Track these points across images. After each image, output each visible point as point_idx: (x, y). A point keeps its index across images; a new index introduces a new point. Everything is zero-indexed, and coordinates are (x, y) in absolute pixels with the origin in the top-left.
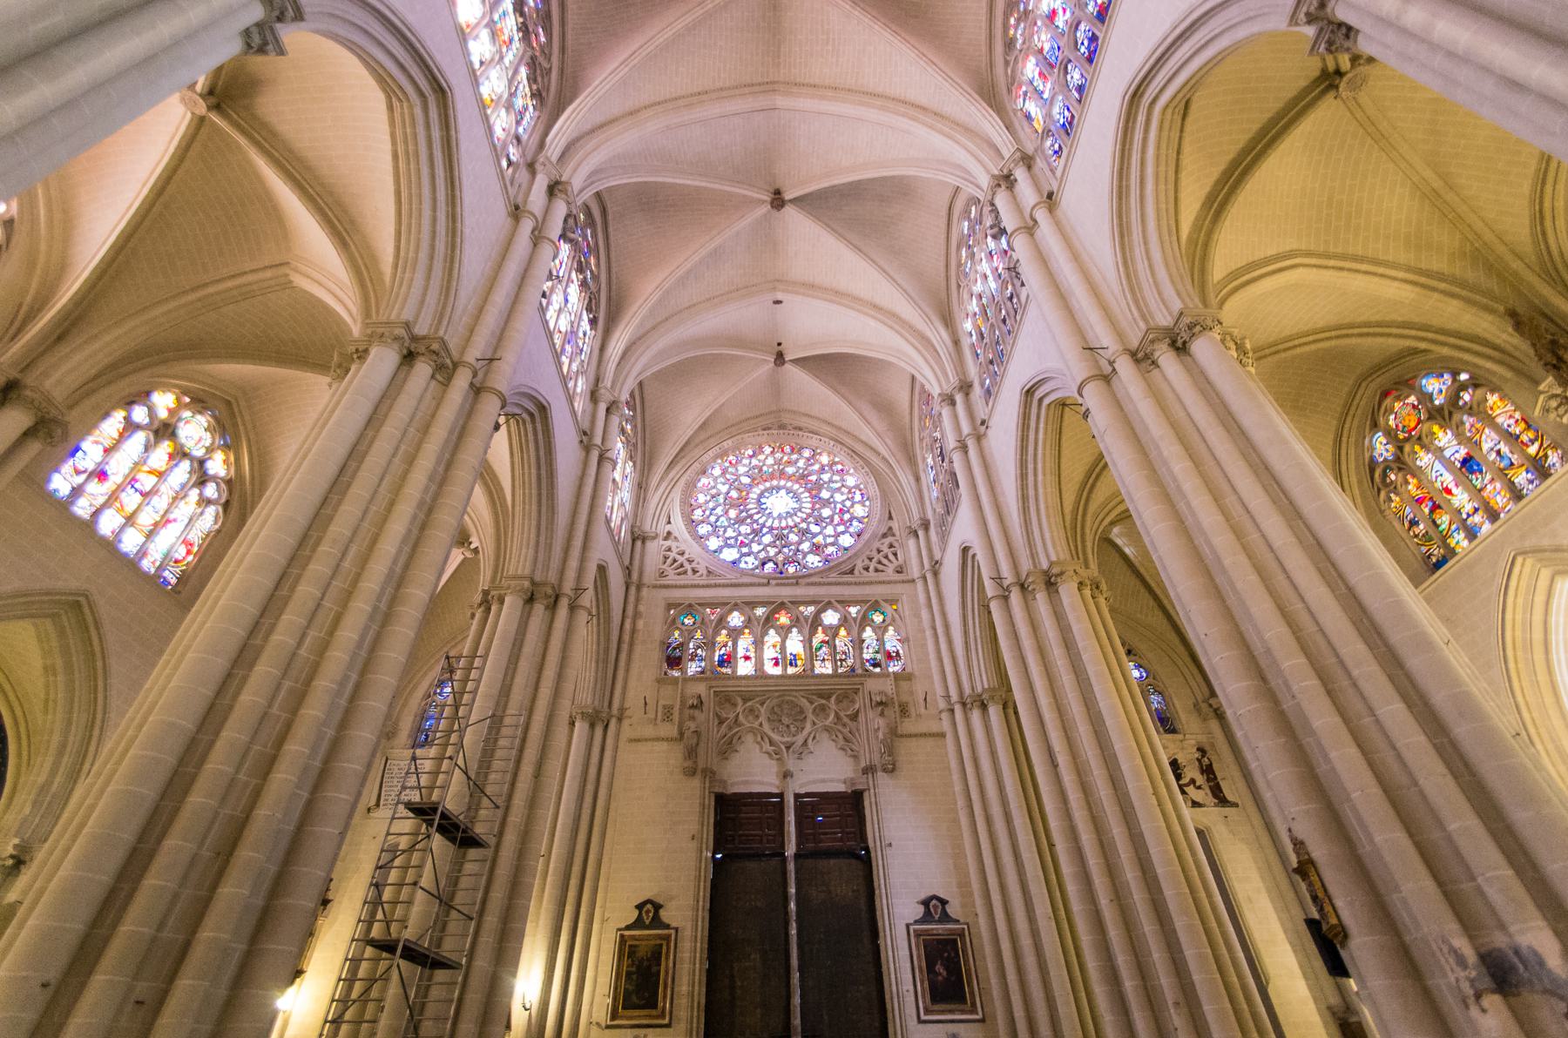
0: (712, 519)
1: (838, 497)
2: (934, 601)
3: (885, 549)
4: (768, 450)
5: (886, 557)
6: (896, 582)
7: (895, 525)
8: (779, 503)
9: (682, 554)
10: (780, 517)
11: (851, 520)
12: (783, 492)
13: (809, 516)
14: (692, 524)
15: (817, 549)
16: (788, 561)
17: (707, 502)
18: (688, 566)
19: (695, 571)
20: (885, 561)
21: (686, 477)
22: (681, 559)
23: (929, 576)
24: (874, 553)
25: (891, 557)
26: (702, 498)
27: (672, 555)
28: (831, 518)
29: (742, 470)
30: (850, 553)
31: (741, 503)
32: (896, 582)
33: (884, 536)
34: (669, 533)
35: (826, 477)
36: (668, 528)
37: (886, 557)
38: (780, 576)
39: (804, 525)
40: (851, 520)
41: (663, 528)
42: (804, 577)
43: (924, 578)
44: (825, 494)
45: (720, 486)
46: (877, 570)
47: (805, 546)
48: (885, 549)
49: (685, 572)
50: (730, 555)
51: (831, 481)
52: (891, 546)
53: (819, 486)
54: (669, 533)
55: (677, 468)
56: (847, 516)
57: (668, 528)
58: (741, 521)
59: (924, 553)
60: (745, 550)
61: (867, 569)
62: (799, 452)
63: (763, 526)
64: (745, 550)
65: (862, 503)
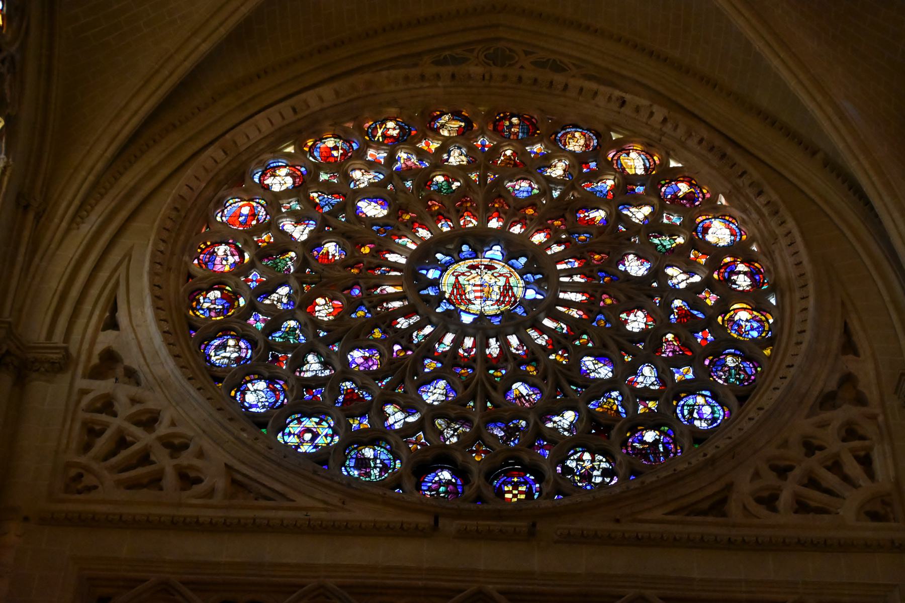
0: (258, 323)
1: (677, 276)
3: (834, 444)
5: (835, 466)
6: (868, 547)
7: (865, 370)
8: (482, 284)
9: (149, 421)
10: (483, 327)
12: (496, 252)
16: (506, 465)
17: (241, 269)
19: (187, 479)
20: (830, 479)
21: (178, 187)
22: (143, 438)
24: (796, 452)
25: (853, 468)
26: (225, 258)
28: (652, 337)
29: (362, 178)
31: (353, 279)
32: (868, 547)
33: (828, 400)
34: (110, 358)
35: (640, 214)
36: (107, 339)
37: (835, 466)
38: (475, 505)
40: (716, 350)
41: (89, 339)
42: (556, 513)
44: (635, 267)
45: (288, 226)
46: (801, 507)
48: (834, 444)
49: (156, 481)
50: (308, 435)
51: (653, 226)
52: (850, 433)
53: (616, 239)
54: (110, 358)
55: (153, 157)
57: (107, 339)
58: (356, 337)
61: (769, 501)
63: (428, 349)
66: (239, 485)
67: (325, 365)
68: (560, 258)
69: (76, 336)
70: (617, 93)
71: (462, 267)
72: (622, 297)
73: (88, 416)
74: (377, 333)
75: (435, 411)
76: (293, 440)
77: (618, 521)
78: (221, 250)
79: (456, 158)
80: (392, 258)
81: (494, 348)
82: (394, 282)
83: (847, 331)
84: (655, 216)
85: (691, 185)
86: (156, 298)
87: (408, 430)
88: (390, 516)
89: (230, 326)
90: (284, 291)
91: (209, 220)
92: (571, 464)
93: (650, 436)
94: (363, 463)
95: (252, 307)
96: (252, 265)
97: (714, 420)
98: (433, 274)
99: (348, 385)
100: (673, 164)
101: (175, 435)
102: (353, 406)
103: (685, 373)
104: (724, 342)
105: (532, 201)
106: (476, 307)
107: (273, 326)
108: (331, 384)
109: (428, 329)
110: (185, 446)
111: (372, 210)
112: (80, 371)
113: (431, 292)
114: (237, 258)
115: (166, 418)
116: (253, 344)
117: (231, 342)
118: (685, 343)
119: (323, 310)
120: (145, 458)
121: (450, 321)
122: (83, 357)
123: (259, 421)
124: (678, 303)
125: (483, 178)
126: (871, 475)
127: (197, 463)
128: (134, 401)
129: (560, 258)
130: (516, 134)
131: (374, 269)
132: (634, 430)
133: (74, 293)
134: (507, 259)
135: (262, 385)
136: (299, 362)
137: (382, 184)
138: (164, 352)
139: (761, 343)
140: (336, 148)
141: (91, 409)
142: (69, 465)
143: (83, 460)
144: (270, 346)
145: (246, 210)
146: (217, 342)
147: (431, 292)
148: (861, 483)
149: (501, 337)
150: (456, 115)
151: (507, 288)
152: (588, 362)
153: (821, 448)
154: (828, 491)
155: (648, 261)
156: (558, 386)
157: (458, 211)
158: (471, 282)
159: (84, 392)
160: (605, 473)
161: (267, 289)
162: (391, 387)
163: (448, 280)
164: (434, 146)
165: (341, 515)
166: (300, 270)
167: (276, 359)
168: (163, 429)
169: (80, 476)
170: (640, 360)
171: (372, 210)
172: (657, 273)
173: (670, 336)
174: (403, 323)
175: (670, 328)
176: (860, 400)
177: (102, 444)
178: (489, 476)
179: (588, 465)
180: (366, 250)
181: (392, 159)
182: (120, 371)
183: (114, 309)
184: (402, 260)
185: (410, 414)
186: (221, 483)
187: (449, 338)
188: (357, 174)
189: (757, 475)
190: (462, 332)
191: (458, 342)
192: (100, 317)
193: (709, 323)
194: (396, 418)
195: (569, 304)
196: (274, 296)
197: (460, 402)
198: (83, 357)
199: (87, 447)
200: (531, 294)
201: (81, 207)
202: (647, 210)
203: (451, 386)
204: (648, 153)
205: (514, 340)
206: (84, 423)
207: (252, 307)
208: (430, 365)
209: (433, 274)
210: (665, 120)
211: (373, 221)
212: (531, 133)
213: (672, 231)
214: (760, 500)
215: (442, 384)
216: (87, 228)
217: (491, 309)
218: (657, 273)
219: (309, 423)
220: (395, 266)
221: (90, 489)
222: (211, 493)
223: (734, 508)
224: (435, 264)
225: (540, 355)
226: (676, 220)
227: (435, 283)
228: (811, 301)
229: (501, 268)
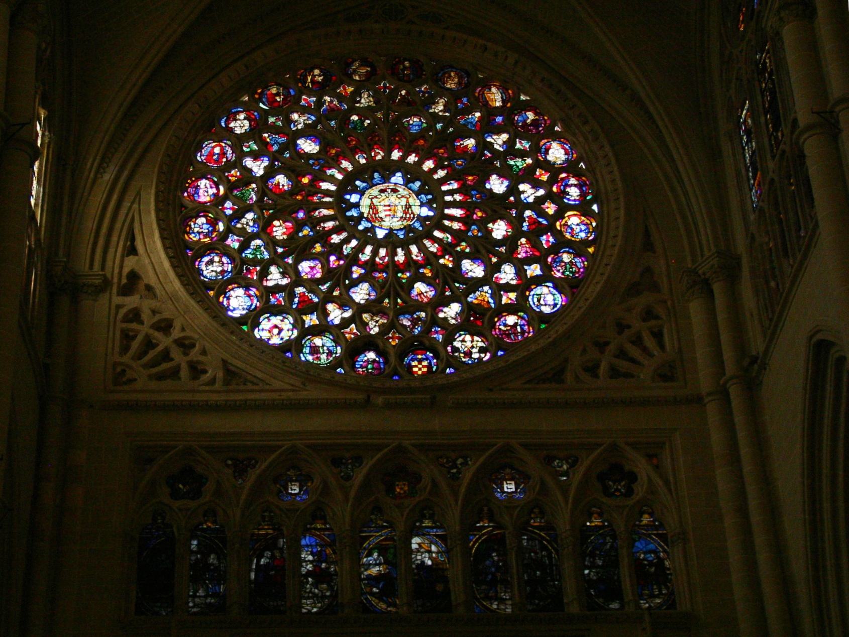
0: (233, 242)
1: (528, 192)
2: (745, 451)
4: (360, 72)
5: (637, 341)
10: (392, 241)
11: (555, 249)
12: (398, 178)
13: (458, 236)
14: (184, 256)
15: (477, 320)
17: (218, 201)
18: (177, 355)
19: (196, 370)
22: (164, 341)
23: (734, 391)
25: (649, 342)
26: (206, 190)
27: (144, 329)
28: (510, 242)
30: (561, 329)
34: (134, 277)
35: (499, 141)
36: (130, 263)
39: (446, 261)
40: (555, 249)
41: (118, 265)
43: (723, 394)
44: (497, 185)
45: (249, 162)
46: (614, 373)
47: (452, 311)
49: (174, 373)
50: (275, 330)
51: (510, 150)
52: (649, 314)
53: (483, 164)
54: (134, 277)
56: (547, 240)
58: (304, 253)
59: (725, 337)
60: (311, 320)
61: (592, 370)
62: (437, 81)
63: (353, 259)
64: (311, 320)
65: (582, 208)
66: (231, 374)
67: (284, 274)
68: (443, 181)
69: (109, 263)
70: (481, 42)
71: (374, 191)
72: (489, 212)
73: (124, 325)
74: (318, 248)
75: (360, 309)
76: (265, 335)
77: (491, 390)
78: (203, 183)
79: (365, 100)
80: (325, 186)
81: (400, 257)
82: (327, 206)
83: (647, 234)
84: (510, 143)
85: (536, 114)
86: (161, 230)
87: (345, 323)
88: (337, 394)
89: (217, 246)
90: (250, 216)
91: (192, 161)
92: (457, 344)
93: (511, 320)
94: (315, 350)
95: (229, 231)
96: (226, 198)
97: (555, 305)
98: (354, 198)
99: (300, 290)
100: (523, 98)
101: (184, 338)
102: (307, 307)
103: (534, 270)
104: (562, 243)
105: (422, 134)
106: (387, 223)
107: (244, 246)
108: (289, 291)
109: (354, 243)
110: (193, 346)
111: (308, 146)
112: (115, 290)
113: (354, 213)
114: (215, 191)
115: (177, 325)
116: (232, 260)
117: (217, 259)
118: (535, 244)
119: (280, 230)
120: (166, 356)
121: (367, 237)
122: (115, 280)
123: (242, 320)
124: (528, 213)
125: (386, 116)
126: (662, 346)
127: (202, 358)
128: (154, 312)
129: (443, 181)
130: (408, 75)
131: (313, 196)
132: (500, 316)
133: (104, 230)
134: (407, 182)
135: (240, 292)
136: (264, 274)
137: (314, 125)
138: (171, 274)
139: (585, 243)
140: (278, 94)
141: (126, 319)
142: (115, 364)
143: (126, 359)
144: (244, 261)
145: (217, 150)
146: (206, 259)
147: (354, 213)
148: (656, 353)
149: (406, 247)
150: (365, 62)
151: (408, 207)
152: (466, 264)
153: (629, 327)
154: (633, 361)
155: (507, 179)
156: (445, 283)
157: (369, 145)
158: (382, 202)
159: (119, 307)
160: (482, 350)
161: (238, 215)
162: (331, 290)
163: (365, 202)
164: (350, 89)
165: (303, 395)
166: (260, 200)
167: (248, 270)
168: (176, 333)
169: (124, 371)
170: (503, 260)
171: (308, 146)
172: (513, 190)
173: (523, 240)
174: (336, 239)
175: (524, 234)
176: (655, 288)
177: (135, 345)
178: (401, 356)
179: (469, 344)
180: (305, 180)
181: (320, 103)
182: (141, 287)
183: (133, 239)
184: (333, 188)
185: (345, 311)
186: (220, 375)
187: (368, 249)
188: (295, 116)
189: (584, 350)
190: (377, 244)
191: (375, 253)
192: (125, 245)
193: (551, 228)
194: (336, 314)
195: (452, 218)
196: (244, 221)
197: (379, 300)
198: (115, 280)
199: (125, 349)
200: (425, 212)
201: (103, 159)
202: (505, 137)
203: (372, 286)
204: (503, 89)
205: (414, 249)
206: (122, 331)
207: (229, 231)
208: (357, 272)
209: (354, 198)
210: (516, 63)
211: (309, 156)
212: (418, 74)
213: (522, 154)
214: (586, 369)
215: (365, 286)
216: (108, 177)
217: (397, 224)
218: (513, 190)
219: (276, 320)
220: (327, 193)
221: (132, 381)
222: (213, 381)
223: (569, 378)
224: (355, 190)
225: (433, 260)
226: (526, 145)
227: (357, 205)
228: (622, 212)
229: (403, 191)
